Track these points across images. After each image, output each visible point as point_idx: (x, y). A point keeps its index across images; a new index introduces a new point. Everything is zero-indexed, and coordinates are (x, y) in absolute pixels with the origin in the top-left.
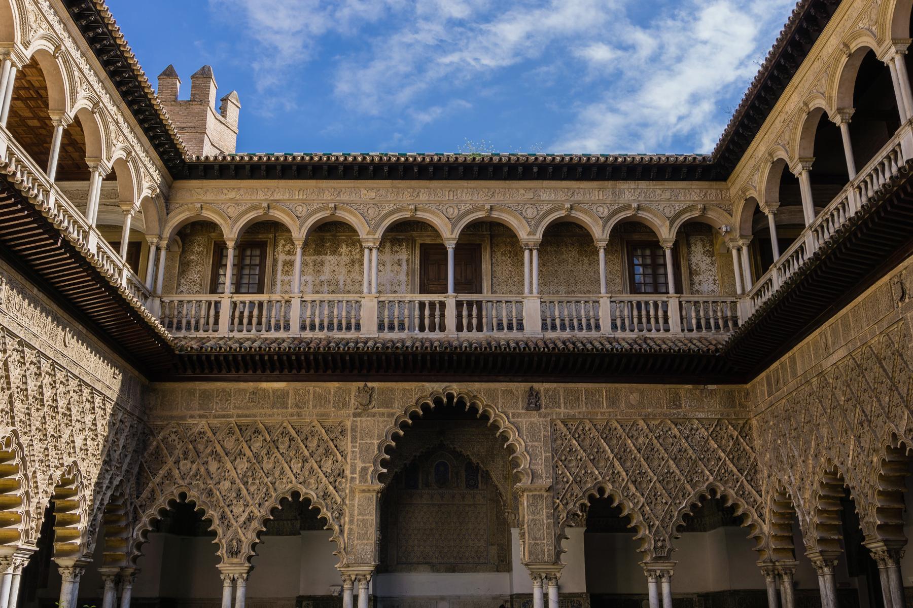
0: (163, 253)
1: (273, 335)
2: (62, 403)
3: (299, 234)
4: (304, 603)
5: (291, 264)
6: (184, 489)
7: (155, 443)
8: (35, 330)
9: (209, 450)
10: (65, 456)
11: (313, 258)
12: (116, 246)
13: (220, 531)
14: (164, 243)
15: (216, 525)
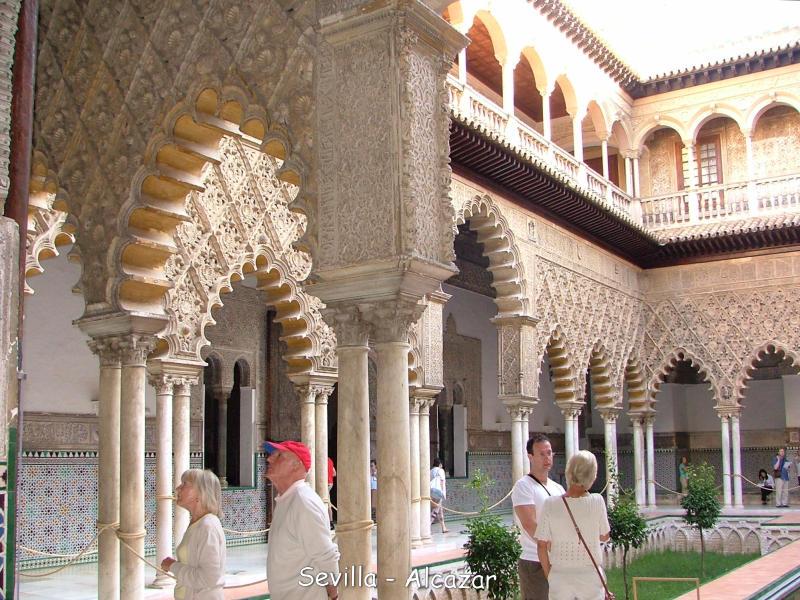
0: (636, 162)
1: (734, 218)
2: (584, 300)
3: (746, 123)
4: (791, 434)
5: (744, 150)
6: (681, 351)
7: (653, 317)
8: (558, 253)
9: (696, 319)
10: (592, 337)
11: (763, 141)
12: (600, 171)
13: (714, 380)
14: (635, 155)
15: (710, 375)
